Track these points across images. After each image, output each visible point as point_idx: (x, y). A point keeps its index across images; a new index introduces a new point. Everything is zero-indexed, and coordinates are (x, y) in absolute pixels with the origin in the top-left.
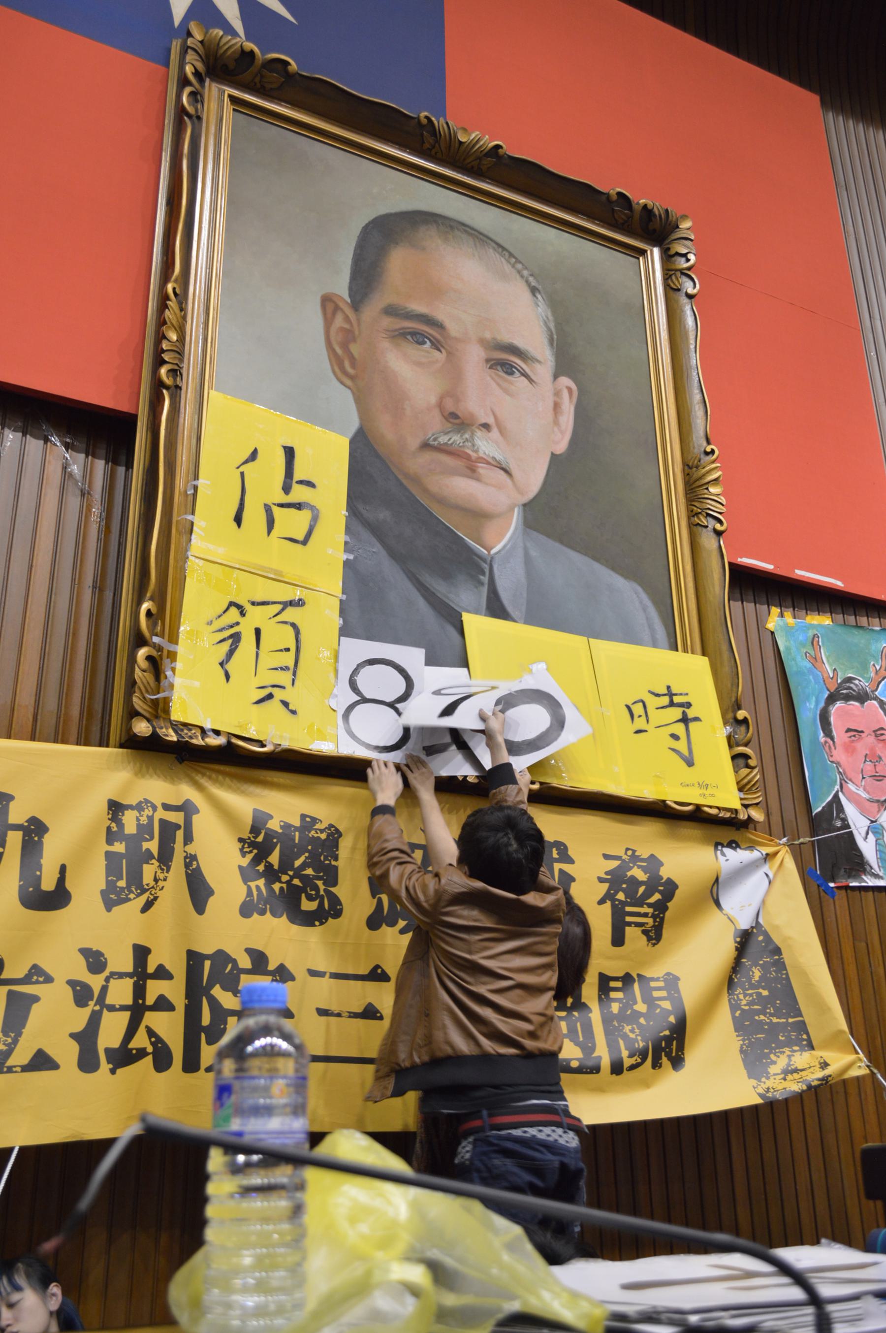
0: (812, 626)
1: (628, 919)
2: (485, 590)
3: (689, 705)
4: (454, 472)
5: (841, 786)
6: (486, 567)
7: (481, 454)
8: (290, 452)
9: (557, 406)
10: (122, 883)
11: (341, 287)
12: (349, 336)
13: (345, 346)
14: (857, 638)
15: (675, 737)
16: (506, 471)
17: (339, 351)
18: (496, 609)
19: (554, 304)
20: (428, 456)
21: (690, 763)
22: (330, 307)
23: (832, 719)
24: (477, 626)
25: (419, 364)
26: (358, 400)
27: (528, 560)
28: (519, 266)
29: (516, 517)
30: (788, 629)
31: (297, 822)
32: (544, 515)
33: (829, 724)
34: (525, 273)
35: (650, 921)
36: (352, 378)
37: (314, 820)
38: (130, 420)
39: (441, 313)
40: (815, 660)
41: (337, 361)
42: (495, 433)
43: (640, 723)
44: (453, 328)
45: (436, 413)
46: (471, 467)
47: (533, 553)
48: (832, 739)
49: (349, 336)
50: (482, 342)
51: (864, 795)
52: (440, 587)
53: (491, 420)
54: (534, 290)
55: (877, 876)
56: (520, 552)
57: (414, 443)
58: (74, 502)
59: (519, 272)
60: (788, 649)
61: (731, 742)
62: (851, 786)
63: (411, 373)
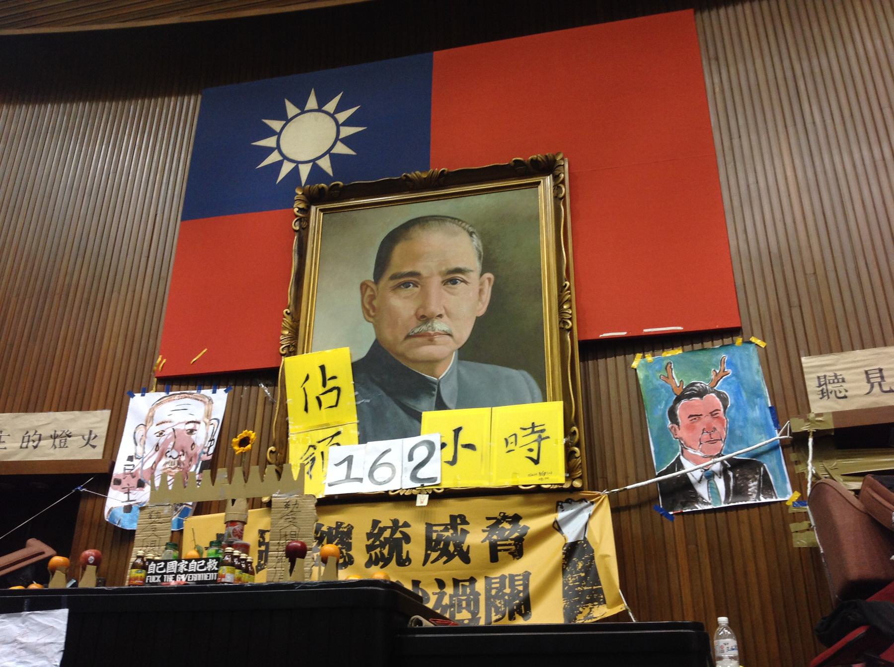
0: (663, 359)
1: (499, 548)
2: (434, 398)
3: (543, 431)
4: (424, 344)
5: (682, 452)
6: (436, 386)
7: (437, 331)
8: (323, 368)
9: (481, 291)
10: (262, 562)
11: (369, 276)
12: (373, 297)
13: (370, 303)
14: (702, 357)
15: (531, 450)
16: (449, 335)
17: (367, 306)
18: (441, 405)
19: (483, 236)
20: (409, 341)
21: (536, 462)
22: (364, 287)
23: (678, 412)
24: (430, 418)
25: (406, 298)
26: (375, 327)
28: (464, 224)
29: (454, 356)
30: (648, 366)
31: (334, 526)
32: (470, 352)
33: (676, 415)
35: (513, 547)
36: (373, 317)
37: (342, 523)
39: (419, 267)
40: (668, 378)
41: (366, 311)
42: (445, 317)
43: (511, 447)
44: (424, 272)
45: (414, 319)
46: (430, 339)
47: (463, 372)
48: (678, 424)
49: (373, 297)
50: (441, 274)
51: (699, 454)
52: (411, 403)
53: (443, 312)
54: (471, 234)
55: (707, 504)
56: (455, 373)
57: (401, 337)
58: (268, 407)
59: (464, 228)
60: (646, 377)
61: (567, 446)
62: (690, 451)
63: (402, 305)
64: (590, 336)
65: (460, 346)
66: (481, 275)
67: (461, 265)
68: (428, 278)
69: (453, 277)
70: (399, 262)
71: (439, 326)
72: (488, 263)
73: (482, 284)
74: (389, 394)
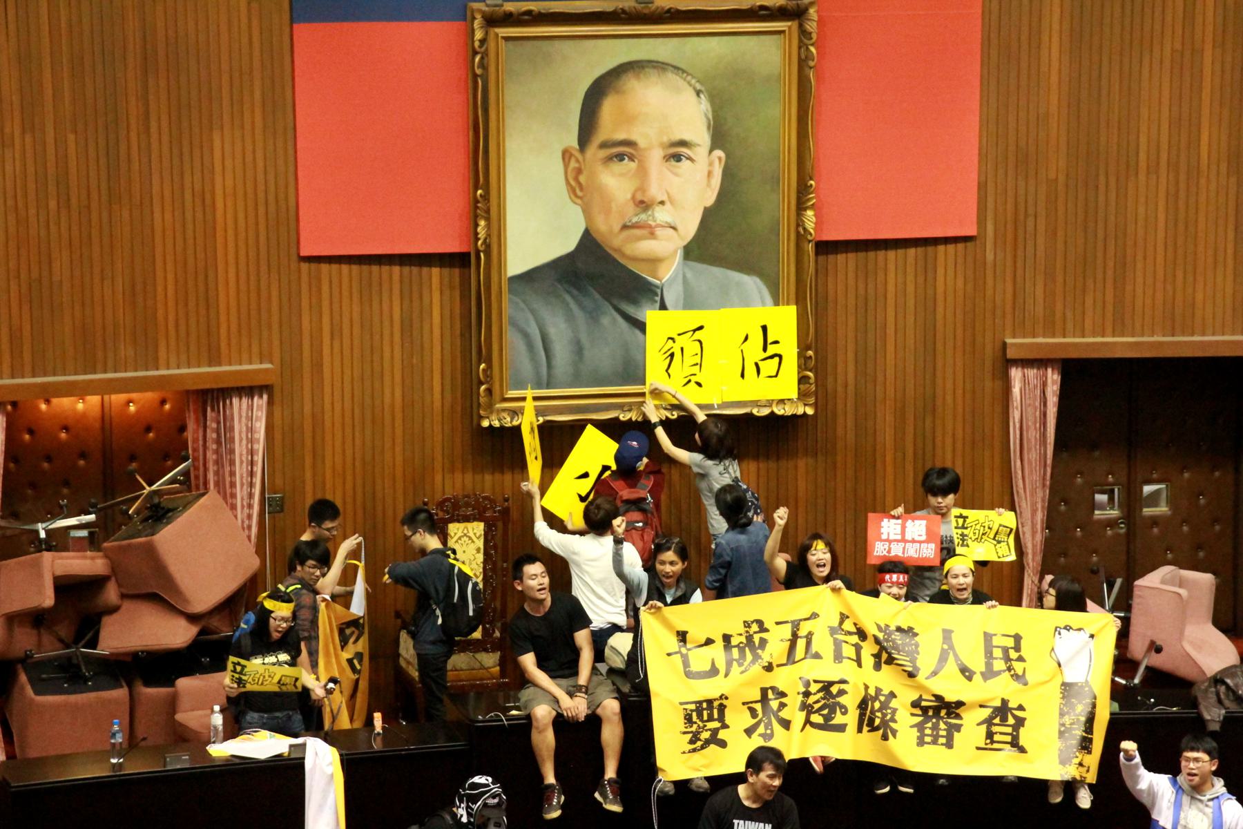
6: (659, 291)
11: (573, 142)
12: (579, 171)
13: (576, 179)
16: (674, 228)
17: (573, 183)
19: (712, 99)
20: (626, 233)
25: (622, 175)
26: (584, 211)
27: (685, 281)
28: (689, 78)
29: (680, 254)
34: (693, 81)
36: (580, 198)
38: (468, 254)
39: (634, 137)
41: (572, 191)
42: (668, 205)
44: (642, 143)
45: (631, 204)
46: (652, 235)
47: (689, 275)
52: (631, 310)
53: (665, 198)
56: (681, 277)
57: (617, 227)
58: (447, 292)
63: (616, 183)
64: (825, 238)
65: (685, 243)
66: (710, 152)
67: (686, 137)
68: (645, 149)
69: (677, 152)
70: (609, 126)
71: (661, 215)
72: (719, 137)
73: (711, 164)
74: (608, 296)
